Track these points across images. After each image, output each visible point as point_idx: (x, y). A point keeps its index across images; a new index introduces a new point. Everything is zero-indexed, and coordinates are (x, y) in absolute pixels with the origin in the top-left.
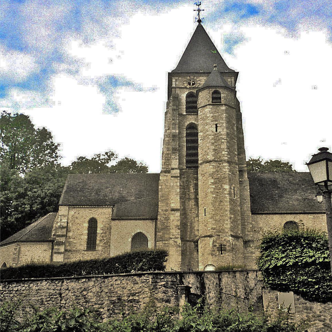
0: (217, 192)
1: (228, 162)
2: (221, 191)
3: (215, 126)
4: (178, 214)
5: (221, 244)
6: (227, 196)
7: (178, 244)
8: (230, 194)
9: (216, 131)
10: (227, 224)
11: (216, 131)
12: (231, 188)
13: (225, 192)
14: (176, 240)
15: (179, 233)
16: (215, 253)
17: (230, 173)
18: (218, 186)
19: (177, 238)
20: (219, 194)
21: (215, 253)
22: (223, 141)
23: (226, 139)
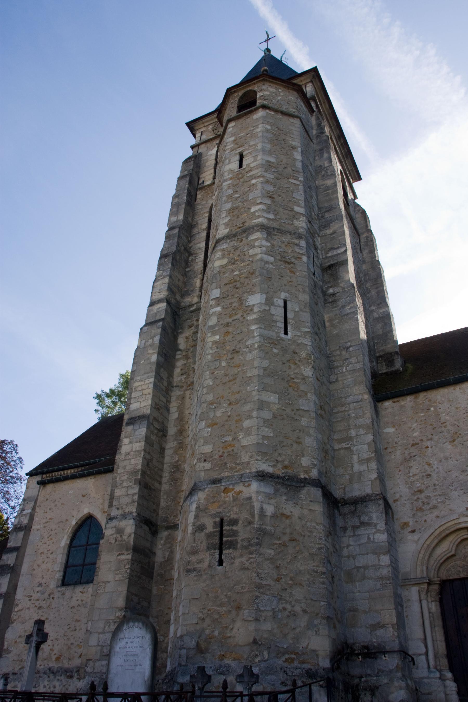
0: (228, 325)
1: (267, 230)
2: (238, 316)
3: (238, 157)
4: (142, 431)
5: (222, 520)
6: (254, 327)
7: (125, 538)
8: (265, 320)
9: (241, 166)
10: (248, 432)
11: (241, 166)
12: (269, 302)
13: (251, 317)
14: (123, 523)
15: (136, 497)
16: (200, 562)
17: (271, 259)
18: (231, 304)
19: (124, 516)
20: (230, 329)
21: (200, 562)
22: (254, 181)
23: (263, 176)
